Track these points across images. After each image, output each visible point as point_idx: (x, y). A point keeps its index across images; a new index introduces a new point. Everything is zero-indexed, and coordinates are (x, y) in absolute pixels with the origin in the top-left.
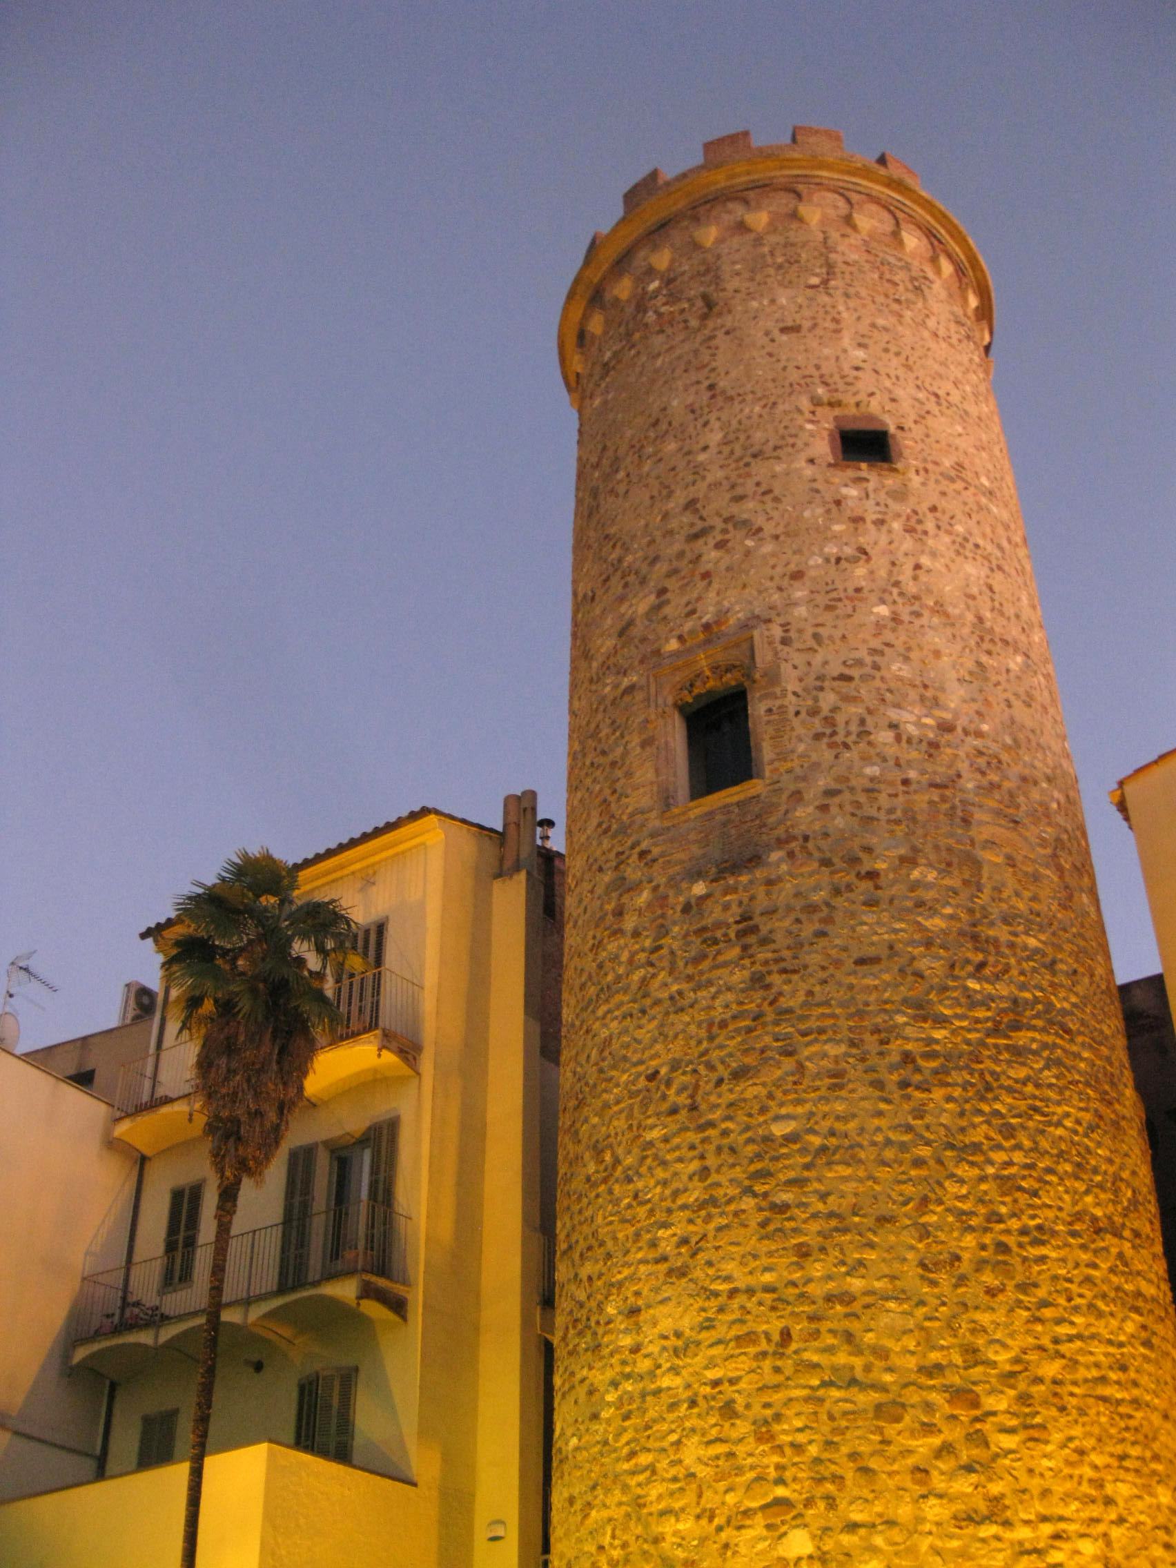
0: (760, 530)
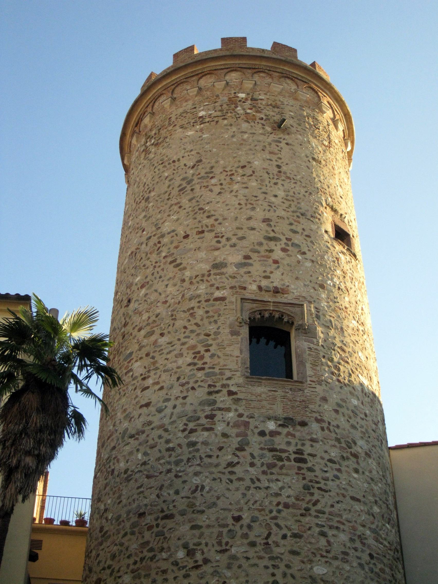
0: (304, 253)
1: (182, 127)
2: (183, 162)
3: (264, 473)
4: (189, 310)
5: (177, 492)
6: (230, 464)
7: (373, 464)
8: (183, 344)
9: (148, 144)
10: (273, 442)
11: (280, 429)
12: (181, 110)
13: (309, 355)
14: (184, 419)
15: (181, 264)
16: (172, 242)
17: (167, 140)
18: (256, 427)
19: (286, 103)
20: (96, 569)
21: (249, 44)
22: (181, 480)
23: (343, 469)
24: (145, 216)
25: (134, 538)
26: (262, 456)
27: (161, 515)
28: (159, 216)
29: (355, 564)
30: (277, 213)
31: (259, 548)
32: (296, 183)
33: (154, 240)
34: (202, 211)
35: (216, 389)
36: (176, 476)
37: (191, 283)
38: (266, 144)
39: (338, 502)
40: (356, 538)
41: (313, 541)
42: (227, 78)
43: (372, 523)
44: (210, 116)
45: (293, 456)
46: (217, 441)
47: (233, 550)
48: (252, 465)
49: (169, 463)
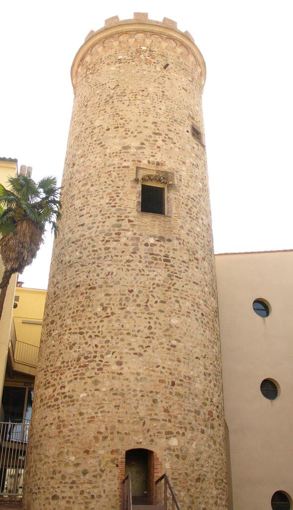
0: (175, 143)
1: (108, 64)
2: (108, 85)
3: (147, 266)
4: (108, 172)
5: (98, 275)
6: (128, 261)
7: (206, 264)
8: (104, 191)
9: (88, 73)
10: (152, 249)
11: (156, 243)
12: (108, 54)
13: (175, 201)
14: (104, 234)
15: (104, 145)
16: (100, 132)
17: (99, 71)
18: (143, 241)
19: (169, 54)
20: (51, 314)
21: (150, 18)
22: (100, 268)
23: (190, 266)
24: (85, 116)
25: (73, 299)
26: (146, 257)
27: (89, 287)
28: (93, 116)
29: (194, 319)
30: (161, 119)
31: (142, 308)
32: (172, 102)
33: (90, 130)
34: (118, 115)
35: (122, 218)
36: (98, 266)
37: (110, 157)
38: (157, 78)
39: (186, 285)
40: (195, 304)
41: (172, 305)
42: (136, 37)
43: (204, 297)
44: (125, 59)
45: (163, 258)
46: (121, 248)
47: (128, 309)
48: (140, 262)
49: (94, 258)
